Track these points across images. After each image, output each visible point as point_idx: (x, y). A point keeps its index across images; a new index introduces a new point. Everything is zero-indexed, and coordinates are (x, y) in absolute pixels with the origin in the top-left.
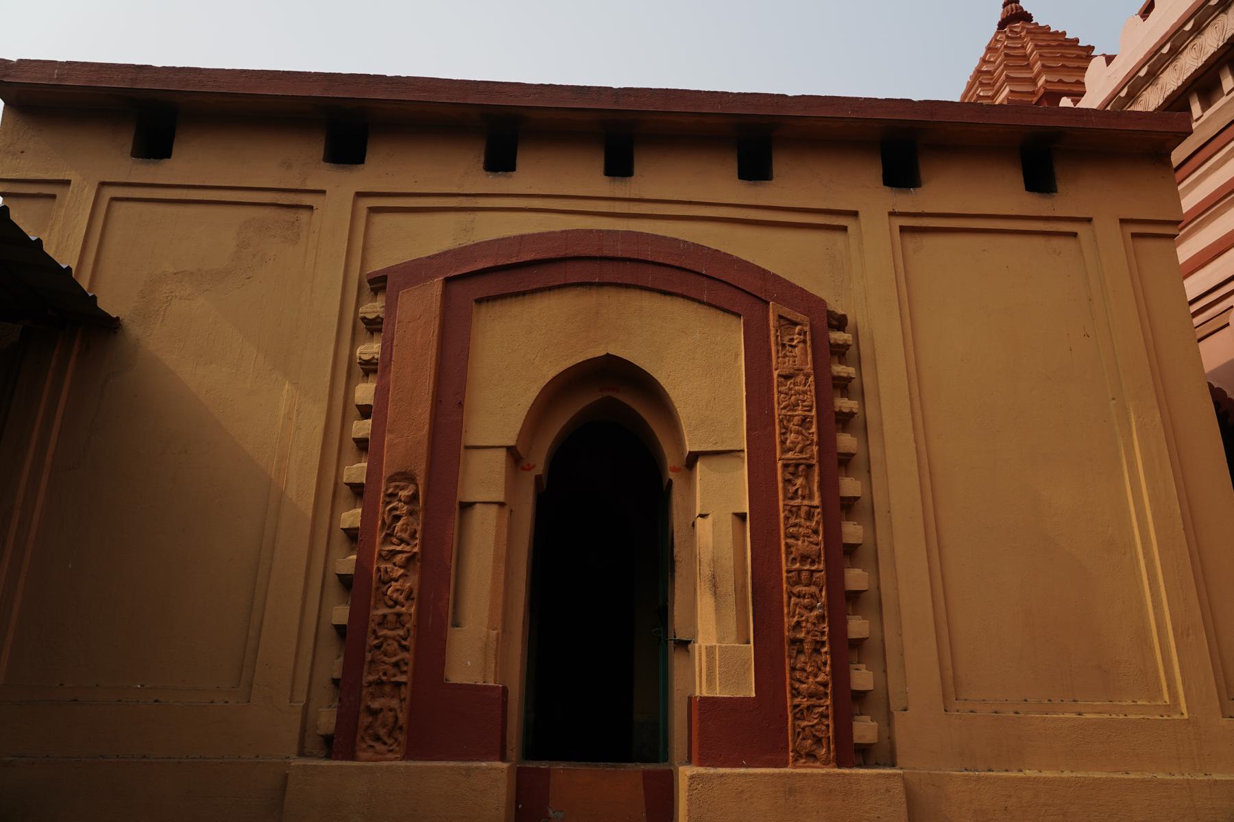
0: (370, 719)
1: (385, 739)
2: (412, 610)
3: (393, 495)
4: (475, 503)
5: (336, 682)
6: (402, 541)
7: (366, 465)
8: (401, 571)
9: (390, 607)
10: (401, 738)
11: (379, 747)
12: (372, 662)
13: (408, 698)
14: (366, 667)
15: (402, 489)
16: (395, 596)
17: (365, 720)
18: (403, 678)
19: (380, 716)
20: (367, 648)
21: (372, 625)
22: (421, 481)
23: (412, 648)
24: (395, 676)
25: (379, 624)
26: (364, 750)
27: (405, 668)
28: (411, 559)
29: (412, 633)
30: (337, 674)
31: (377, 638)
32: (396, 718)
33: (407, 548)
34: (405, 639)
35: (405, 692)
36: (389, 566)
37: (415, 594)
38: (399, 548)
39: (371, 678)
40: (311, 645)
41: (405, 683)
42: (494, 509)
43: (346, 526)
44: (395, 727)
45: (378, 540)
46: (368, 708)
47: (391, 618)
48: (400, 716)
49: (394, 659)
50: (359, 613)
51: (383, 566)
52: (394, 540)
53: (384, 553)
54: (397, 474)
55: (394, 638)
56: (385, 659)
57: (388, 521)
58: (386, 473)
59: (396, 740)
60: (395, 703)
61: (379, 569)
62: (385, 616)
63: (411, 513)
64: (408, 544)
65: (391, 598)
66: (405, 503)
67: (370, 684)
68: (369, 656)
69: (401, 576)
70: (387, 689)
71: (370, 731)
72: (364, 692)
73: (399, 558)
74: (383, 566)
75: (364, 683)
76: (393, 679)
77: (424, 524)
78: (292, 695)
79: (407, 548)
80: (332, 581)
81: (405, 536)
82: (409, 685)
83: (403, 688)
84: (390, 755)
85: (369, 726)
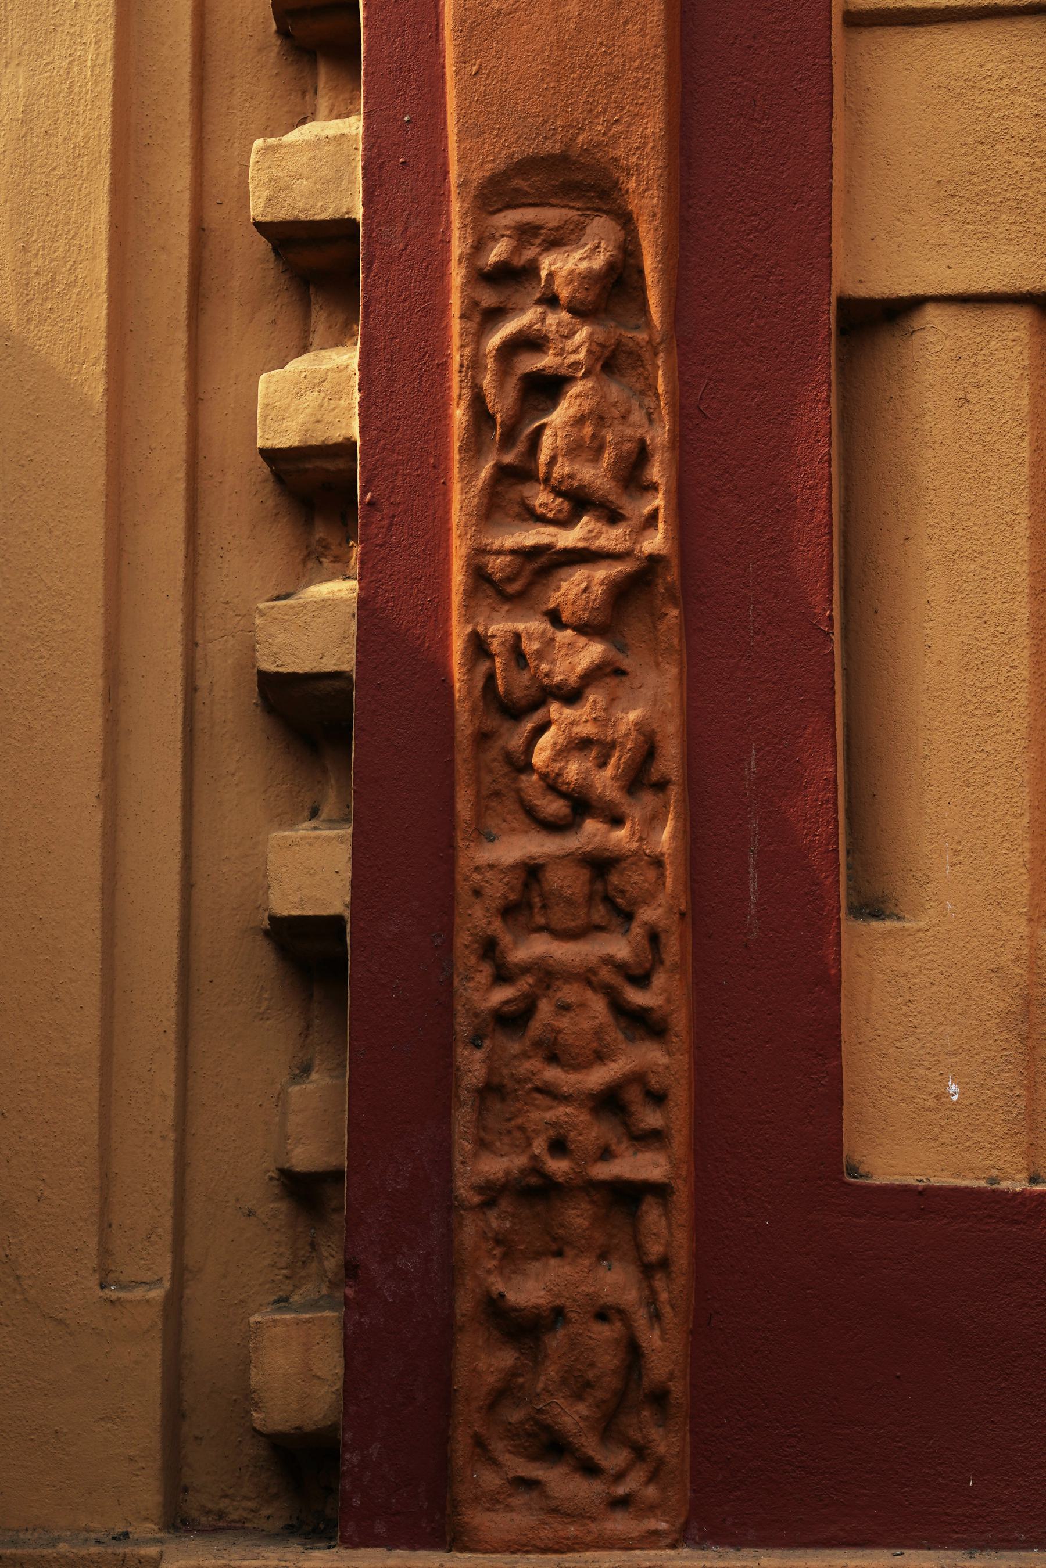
0: (506, 1358)
1: (590, 1446)
2: (665, 838)
3: (511, 276)
4: (916, 303)
5: (303, 1191)
6: (579, 502)
7: (354, 126)
8: (592, 652)
9: (553, 827)
10: (667, 1442)
11: (561, 1482)
12: (492, 1090)
13: (682, 1262)
14: (463, 1117)
15: (555, 242)
16: (573, 770)
17: (484, 1361)
18: (646, 1166)
19: (555, 1341)
20: (463, 1025)
21: (477, 917)
22: (647, 198)
23: (680, 1022)
24: (606, 1154)
25: (508, 911)
26: (494, 1501)
27: (652, 1119)
28: (635, 586)
29: (673, 948)
30: (305, 1156)
31: (503, 976)
32: (633, 1351)
33: (611, 538)
34: (641, 980)
35: (664, 1230)
36: (531, 626)
37: (670, 762)
38: (569, 538)
39: (495, 1166)
40: (170, 1015)
41: (660, 1191)
42: (1012, 334)
43: (284, 435)
44: (631, 1392)
45: (461, 500)
46: (495, 1308)
47: (565, 880)
48: (652, 1339)
49: (598, 1077)
50: (406, 857)
51: (499, 628)
52: (542, 498)
53: (497, 565)
54: (524, 166)
55: (586, 977)
56: (552, 1074)
57: (501, 404)
58: (462, 162)
59: (640, 1452)
60: (617, 1282)
61: (478, 646)
62: (532, 871)
63: (609, 362)
64: (613, 517)
65: (552, 784)
66: (580, 312)
67: (492, 1193)
68: (472, 1065)
69: (593, 675)
70: (577, 1216)
71: (515, 1416)
72: (469, 1232)
73: (577, 588)
74: (499, 628)
75: (463, 1189)
76: (603, 1171)
77: (685, 416)
78: (105, 1251)
79: (611, 538)
80: (231, 707)
81: (595, 475)
82: (682, 1196)
83: (652, 1215)
84: (620, 1524)
85: (505, 1392)
